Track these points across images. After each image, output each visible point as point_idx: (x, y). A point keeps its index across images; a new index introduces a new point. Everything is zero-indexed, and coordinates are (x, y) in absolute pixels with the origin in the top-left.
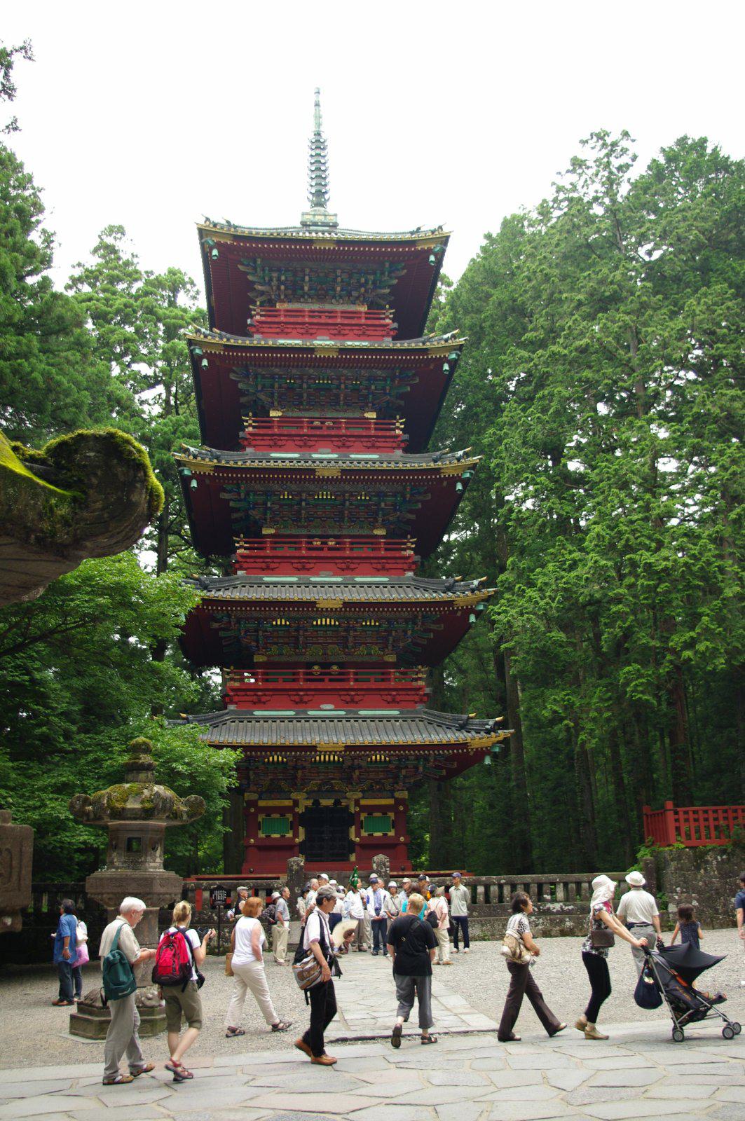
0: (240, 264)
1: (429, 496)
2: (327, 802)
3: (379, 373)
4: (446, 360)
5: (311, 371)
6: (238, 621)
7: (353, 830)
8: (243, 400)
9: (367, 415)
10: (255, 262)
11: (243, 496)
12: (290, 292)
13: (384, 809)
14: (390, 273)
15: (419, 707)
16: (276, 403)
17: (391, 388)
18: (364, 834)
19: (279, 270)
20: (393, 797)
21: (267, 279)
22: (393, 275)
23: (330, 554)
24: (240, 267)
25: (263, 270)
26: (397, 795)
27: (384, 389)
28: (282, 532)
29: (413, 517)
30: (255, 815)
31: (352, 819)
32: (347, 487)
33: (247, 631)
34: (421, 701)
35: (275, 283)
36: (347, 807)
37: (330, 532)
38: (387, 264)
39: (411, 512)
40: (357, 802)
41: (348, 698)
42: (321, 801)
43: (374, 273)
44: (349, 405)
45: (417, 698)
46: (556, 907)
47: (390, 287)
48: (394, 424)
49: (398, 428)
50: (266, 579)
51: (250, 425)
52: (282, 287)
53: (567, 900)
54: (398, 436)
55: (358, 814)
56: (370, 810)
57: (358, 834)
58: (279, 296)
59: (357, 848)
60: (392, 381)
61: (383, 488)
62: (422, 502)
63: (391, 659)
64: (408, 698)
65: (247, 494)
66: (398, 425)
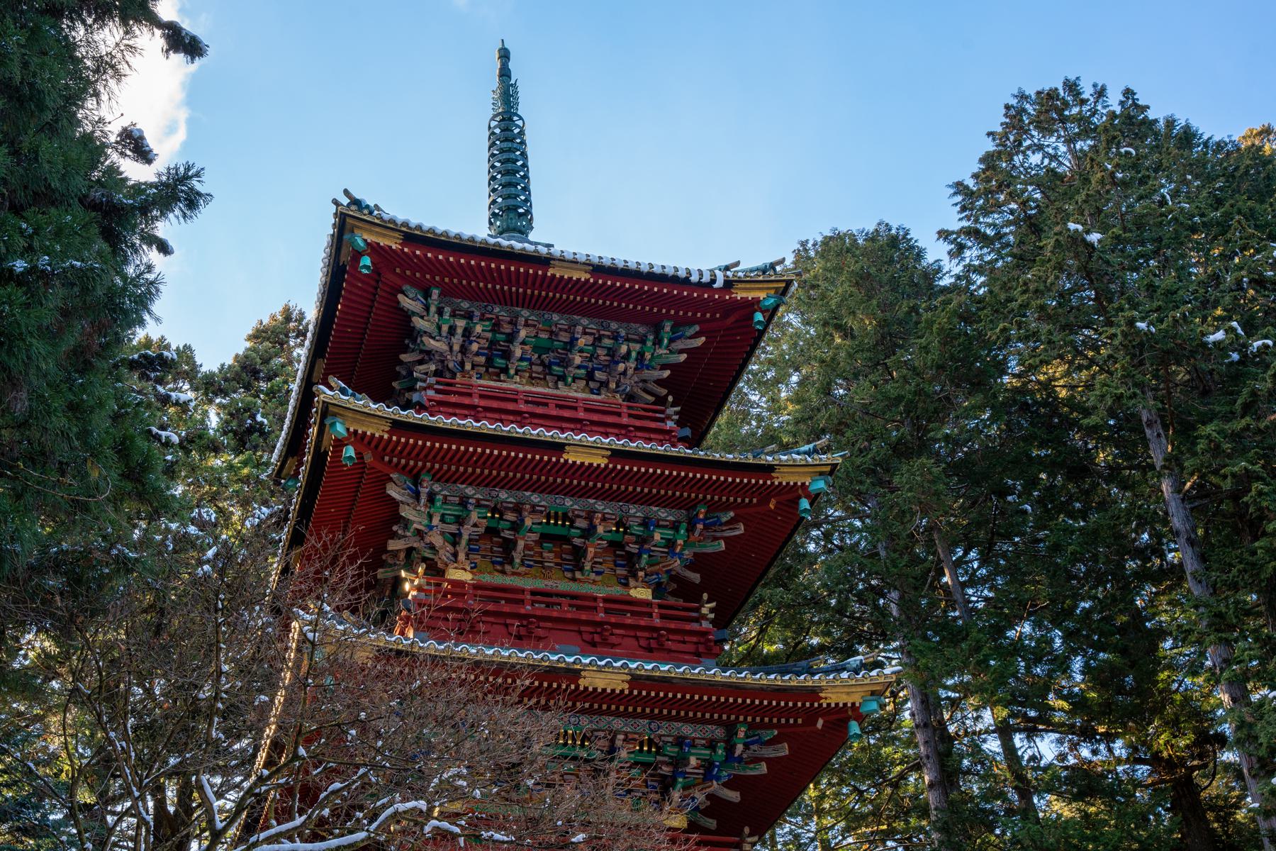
1: (784, 750)
3: (663, 513)
5: (535, 498)
9: (633, 593)
10: (427, 295)
12: (482, 359)
14: (671, 340)
16: (462, 556)
17: (686, 544)
19: (469, 316)
21: (445, 328)
22: (679, 345)
24: (400, 297)
25: (440, 312)
27: (670, 544)
29: (734, 796)
38: (668, 326)
43: (643, 341)
48: (698, 610)
49: (704, 617)
54: (704, 633)
58: (462, 364)
60: (691, 529)
61: (687, 730)
62: (769, 761)
66: (704, 611)
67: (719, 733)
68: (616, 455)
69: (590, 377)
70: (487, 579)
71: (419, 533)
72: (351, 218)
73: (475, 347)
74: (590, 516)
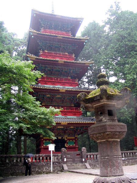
0: (40, 20)
2: (60, 138)
3: (69, 45)
4: (85, 42)
6: (39, 95)
7: (66, 144)
8: (38, 48)
9: (65, 53)
11: (40, 67)
13: (72, 139)
15: (80, 116)
16: (46, 49)
18: (68, 145)
20: (74, 137)
23: (60, 81)
26: (76, 136)
28: (48, 76)
30: (43, 141)
31: (65, 142)
32: (63, 67)
33: (41, 97)
34: (81, 115)
35: (46, 25)
36: (64, 139)
37: (59, 77)
39: (76, 74)
40: (67, 138)
41: (65, 114)
42: (58, 137)
44: (62, 51)
45: (80, 114)
46: (123, 159)
47: (71, 28)
50: (45, 86)
51: (41, 52)
52: (48, 26)
53: (125, 157)
54: (73, 58)
55: (67, 140)
56: (69, 140)
57: (67, 145)
59: (67, 149)
62: (80, 71)
63: (73, 105)
64: (78, 114)
65: (41, 67)
67: (74, 68)
68: (64, 37)
69: (61, 30)
70: (49, 52)
71: (41, 47)
72: (33, 10)
73: (48, 26)
74: (61, 44)
